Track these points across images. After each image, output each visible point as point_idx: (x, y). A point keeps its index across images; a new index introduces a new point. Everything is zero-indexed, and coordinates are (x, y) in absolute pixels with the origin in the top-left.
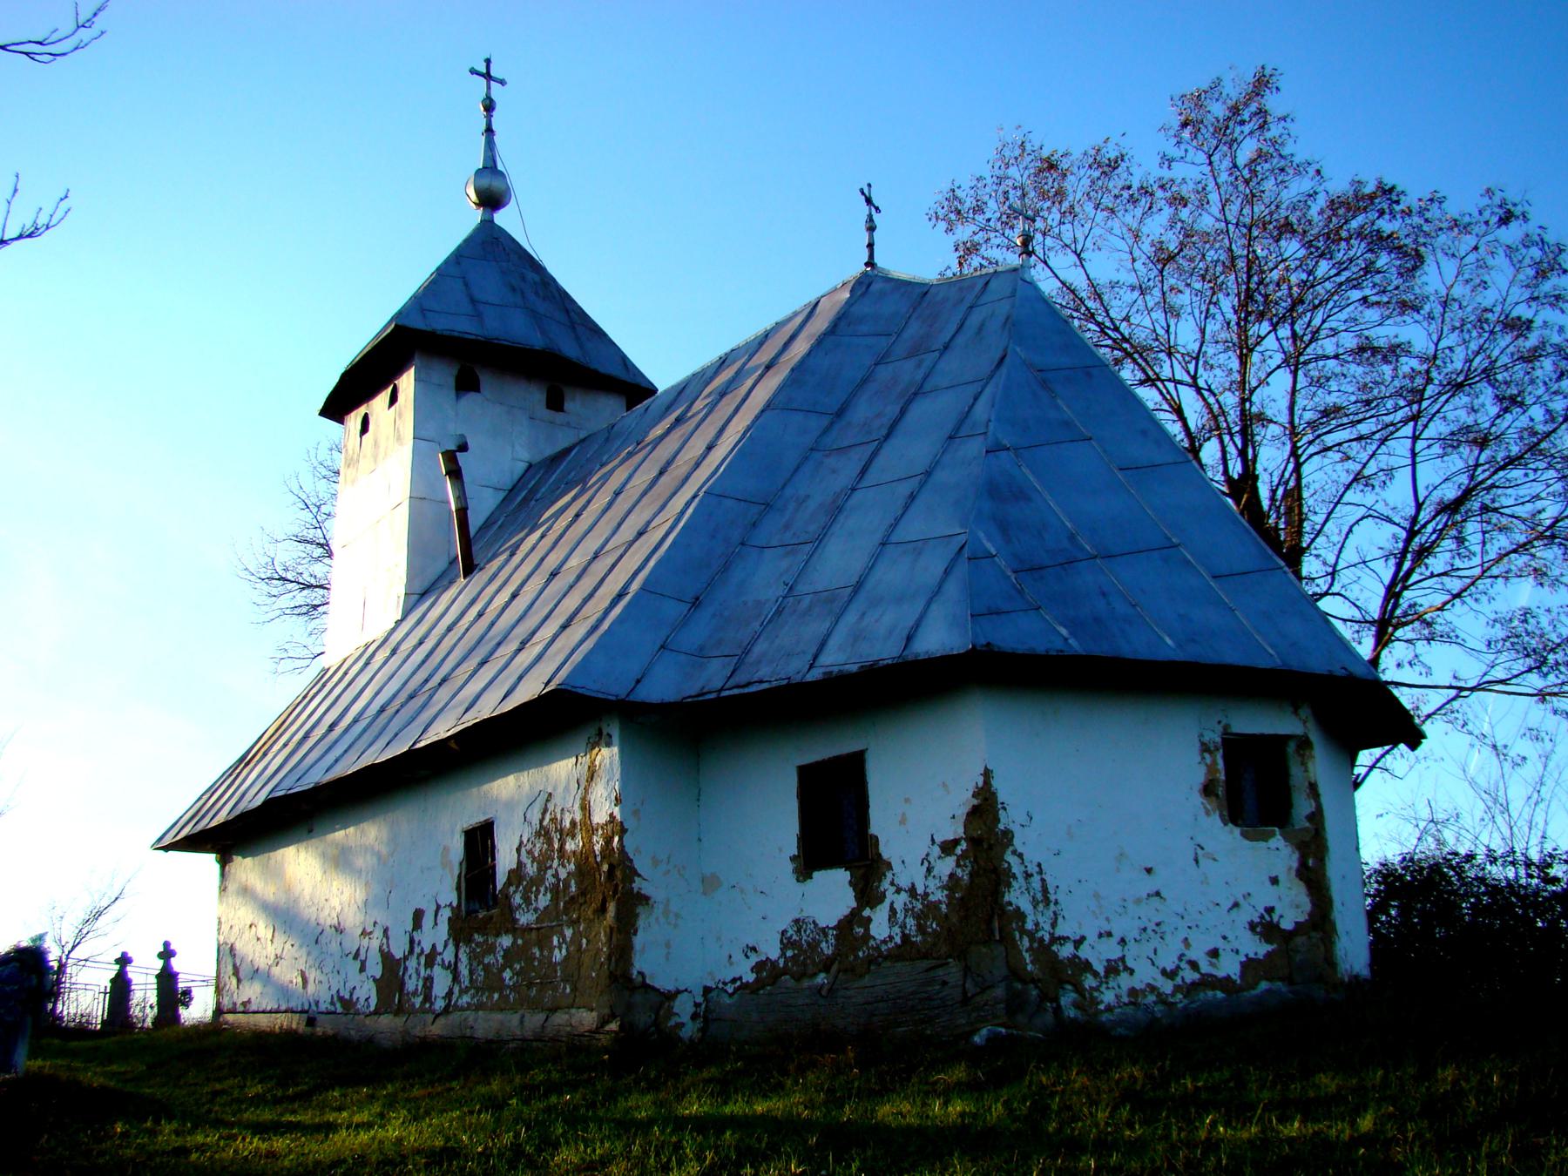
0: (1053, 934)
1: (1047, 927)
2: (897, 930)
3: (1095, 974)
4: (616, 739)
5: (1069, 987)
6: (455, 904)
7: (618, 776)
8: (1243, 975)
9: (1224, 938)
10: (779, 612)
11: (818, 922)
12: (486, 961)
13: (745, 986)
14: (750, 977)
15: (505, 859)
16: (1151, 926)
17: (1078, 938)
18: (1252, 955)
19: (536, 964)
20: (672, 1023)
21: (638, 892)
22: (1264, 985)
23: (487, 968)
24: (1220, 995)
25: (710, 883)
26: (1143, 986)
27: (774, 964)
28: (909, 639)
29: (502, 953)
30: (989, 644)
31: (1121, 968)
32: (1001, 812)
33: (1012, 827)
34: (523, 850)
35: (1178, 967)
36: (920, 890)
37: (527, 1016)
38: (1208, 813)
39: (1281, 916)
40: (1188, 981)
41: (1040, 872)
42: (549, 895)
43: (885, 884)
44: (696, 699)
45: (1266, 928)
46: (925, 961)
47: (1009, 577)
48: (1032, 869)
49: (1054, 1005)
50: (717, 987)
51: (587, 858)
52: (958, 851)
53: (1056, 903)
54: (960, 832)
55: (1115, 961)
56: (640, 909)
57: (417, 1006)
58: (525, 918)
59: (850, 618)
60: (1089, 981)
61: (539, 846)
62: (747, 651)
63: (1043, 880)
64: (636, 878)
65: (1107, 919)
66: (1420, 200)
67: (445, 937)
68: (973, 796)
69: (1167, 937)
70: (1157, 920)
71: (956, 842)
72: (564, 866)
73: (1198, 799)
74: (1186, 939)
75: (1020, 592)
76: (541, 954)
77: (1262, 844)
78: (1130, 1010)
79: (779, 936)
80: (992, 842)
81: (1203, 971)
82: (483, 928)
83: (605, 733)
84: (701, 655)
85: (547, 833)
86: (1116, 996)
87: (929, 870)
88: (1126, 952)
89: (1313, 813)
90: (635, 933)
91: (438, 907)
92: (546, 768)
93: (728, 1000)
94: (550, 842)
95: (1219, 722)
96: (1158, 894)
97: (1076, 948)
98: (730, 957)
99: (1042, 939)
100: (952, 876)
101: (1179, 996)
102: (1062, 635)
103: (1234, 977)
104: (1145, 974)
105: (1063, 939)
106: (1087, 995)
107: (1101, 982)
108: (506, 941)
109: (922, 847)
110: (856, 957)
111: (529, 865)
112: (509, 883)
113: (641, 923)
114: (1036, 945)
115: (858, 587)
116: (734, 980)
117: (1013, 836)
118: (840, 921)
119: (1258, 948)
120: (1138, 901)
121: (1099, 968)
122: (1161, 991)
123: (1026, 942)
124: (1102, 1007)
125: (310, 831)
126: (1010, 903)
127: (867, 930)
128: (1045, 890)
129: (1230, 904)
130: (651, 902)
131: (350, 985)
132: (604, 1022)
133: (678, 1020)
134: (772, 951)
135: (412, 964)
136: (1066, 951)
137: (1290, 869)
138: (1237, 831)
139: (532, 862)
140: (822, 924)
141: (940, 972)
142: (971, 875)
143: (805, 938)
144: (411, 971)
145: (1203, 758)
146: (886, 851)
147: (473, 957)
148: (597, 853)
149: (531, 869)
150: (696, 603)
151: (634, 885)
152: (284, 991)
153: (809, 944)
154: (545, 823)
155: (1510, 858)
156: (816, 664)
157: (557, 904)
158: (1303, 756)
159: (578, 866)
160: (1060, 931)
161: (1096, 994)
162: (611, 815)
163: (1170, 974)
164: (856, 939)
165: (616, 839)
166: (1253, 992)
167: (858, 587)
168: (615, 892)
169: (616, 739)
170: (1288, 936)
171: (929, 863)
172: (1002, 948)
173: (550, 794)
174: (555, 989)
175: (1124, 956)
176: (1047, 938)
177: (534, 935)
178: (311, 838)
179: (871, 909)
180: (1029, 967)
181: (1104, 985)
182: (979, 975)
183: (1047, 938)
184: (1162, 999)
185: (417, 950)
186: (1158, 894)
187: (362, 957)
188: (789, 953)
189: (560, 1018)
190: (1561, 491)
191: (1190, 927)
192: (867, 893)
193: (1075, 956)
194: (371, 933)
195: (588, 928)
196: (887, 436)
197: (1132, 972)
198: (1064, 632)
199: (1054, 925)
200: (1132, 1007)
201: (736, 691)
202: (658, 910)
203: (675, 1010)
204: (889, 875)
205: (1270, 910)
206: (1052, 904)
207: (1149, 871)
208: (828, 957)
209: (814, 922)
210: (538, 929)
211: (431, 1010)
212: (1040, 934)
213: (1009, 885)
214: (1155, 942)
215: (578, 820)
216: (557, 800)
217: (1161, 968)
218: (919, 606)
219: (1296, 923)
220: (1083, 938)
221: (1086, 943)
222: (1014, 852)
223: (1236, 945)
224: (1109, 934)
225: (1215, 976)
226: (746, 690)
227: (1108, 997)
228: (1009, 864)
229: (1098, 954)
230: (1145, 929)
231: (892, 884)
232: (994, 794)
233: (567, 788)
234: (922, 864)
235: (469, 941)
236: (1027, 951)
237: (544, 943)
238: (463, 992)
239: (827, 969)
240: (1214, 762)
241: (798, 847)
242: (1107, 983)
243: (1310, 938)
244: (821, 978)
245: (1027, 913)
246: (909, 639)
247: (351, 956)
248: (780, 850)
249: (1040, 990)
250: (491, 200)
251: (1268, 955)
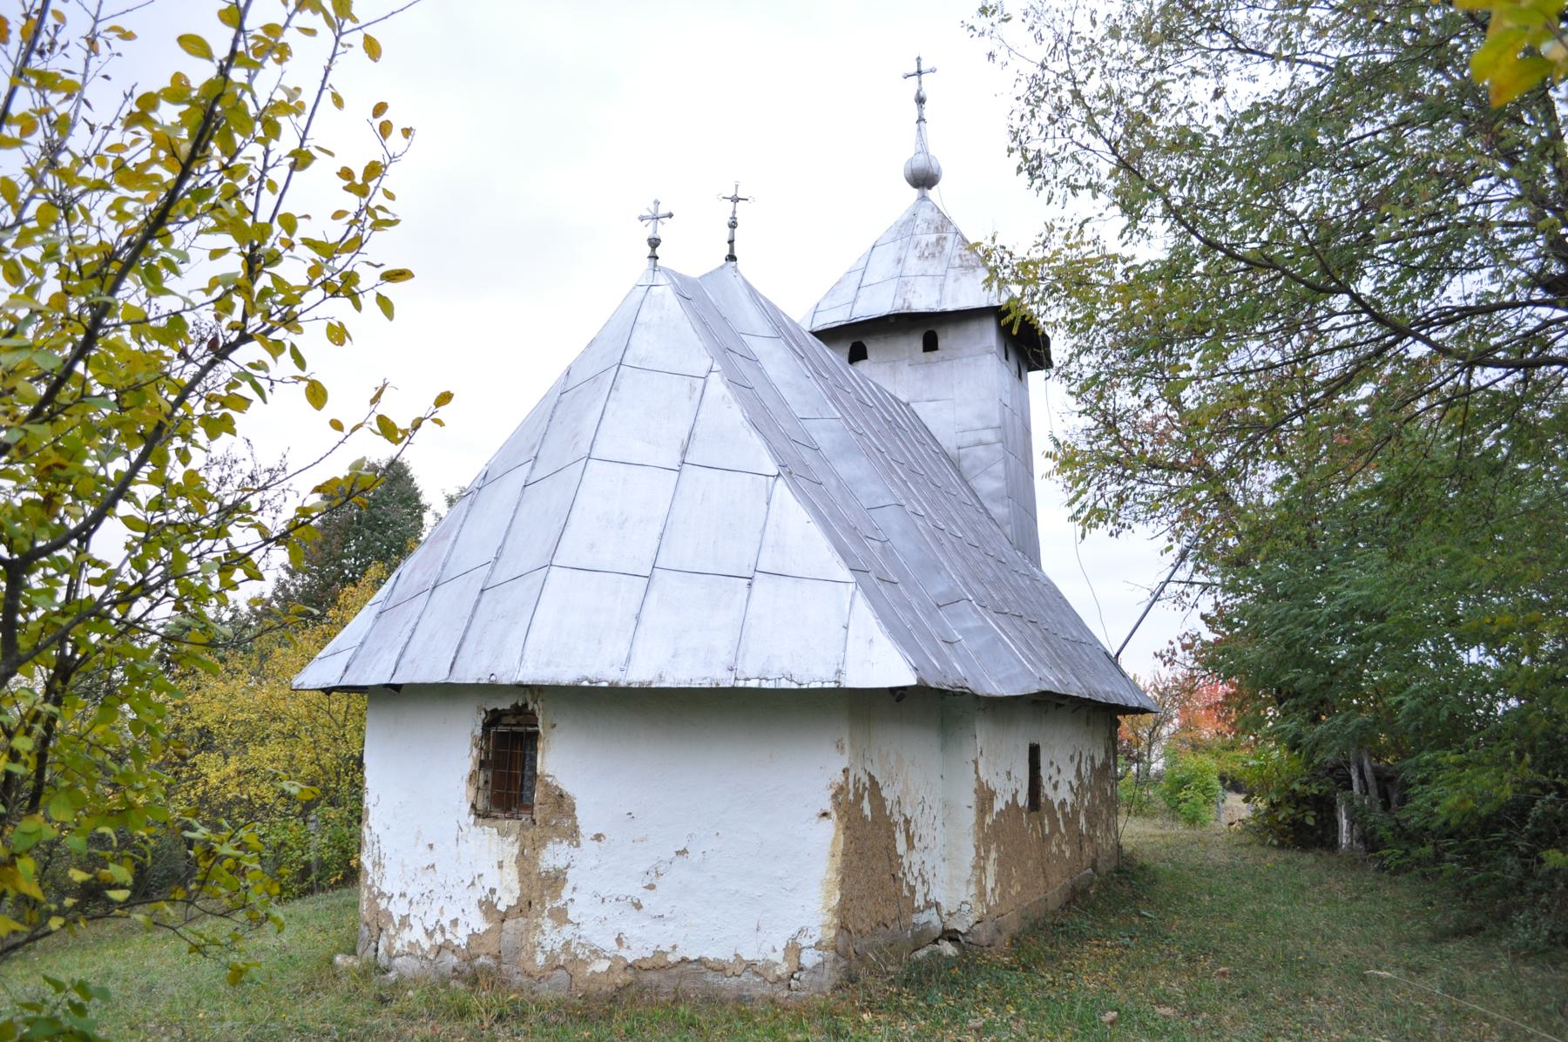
16: (427, 892)
119: (479, 924)
123: (366, 894)
160: (385, 889)
186: (433, 866)
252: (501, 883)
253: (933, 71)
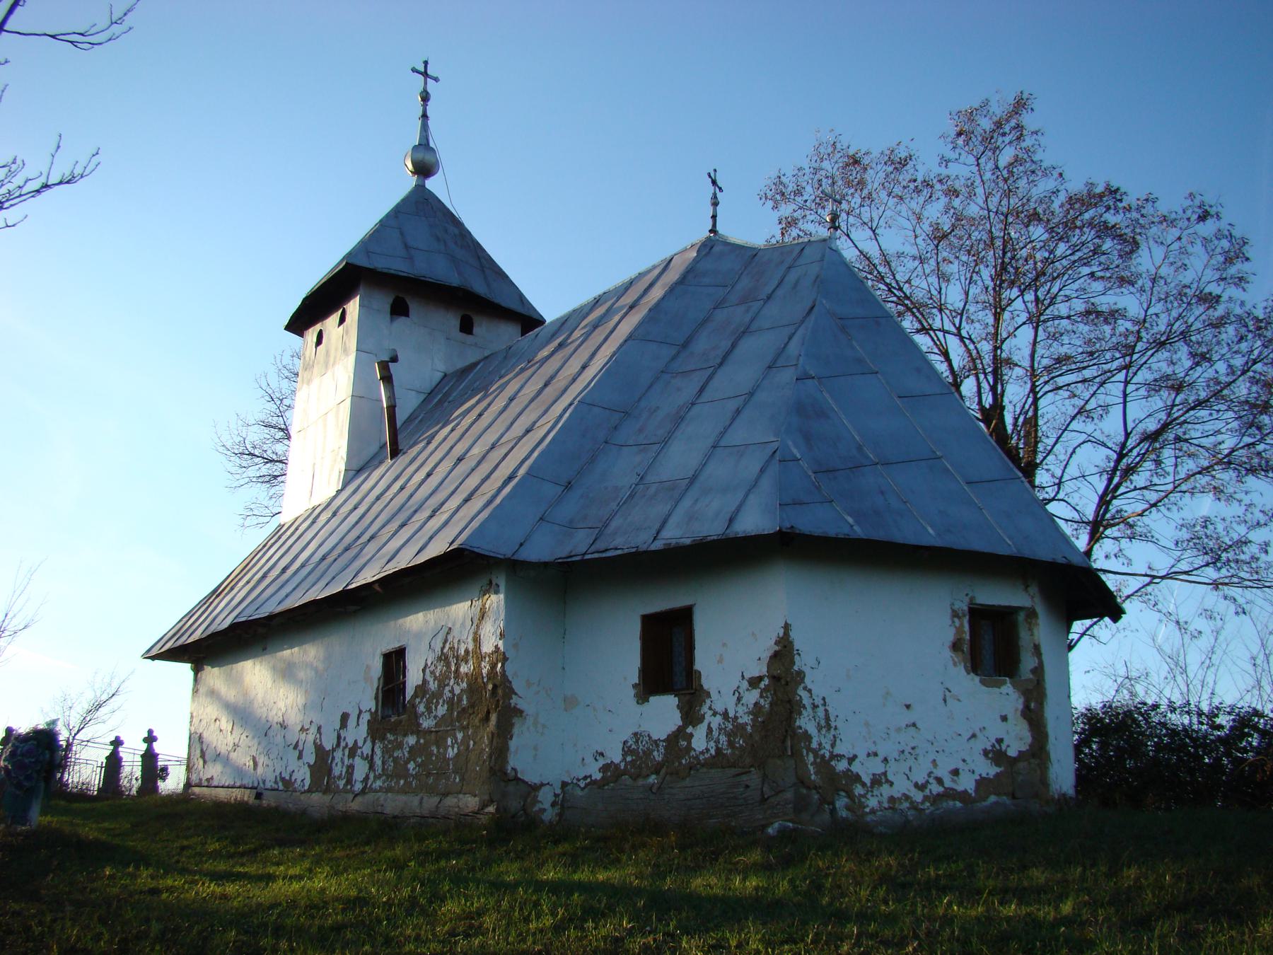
0: (832, 752)
1: (828, 747)
2: (712, 744)
3: (864, 784)
4: (502, 588)
5: (843, 794)
6: (373, 710)
7: (502, 616)
8: (976, 790)
9: (964, 761)
10: (632, 496)
11: (651, 735)
12: (395, 755)
13: (594, 782)
14: (598, 776)
15: (413, 677)
16: (908, 749)
17: (851, 756)
18: (984, 775)
19: (434, 758)
20: (536, 809)
21: (515, 707)
22: (993, 798)
23: (396, 760)
24: (958, 804)
25: (570, 703)
26: (900, 795)
27: (617, 766)
28: (731, 520)
29: (408, 749)
30: (792, 527)
31: (883, 781)
32: (796, 657)
33: (804, 669)
34: (428, 671)
35: (927, 782)
36: (731, 714)
37: (425, 799)
38: (955, 664)
39: (1008, 746)
40: (934, 793)
41: (825, 704)
42: (446, 706)
43: (705, 709)
44: (565, 560)
45: (996, 754)
46: (733, 769)
47: (810, 476)
48: (818, 701)
49: (831, 807)
50: (572, 782)
51: (476, 679)
52: (762, 685)
53: (836, 728)
54: (764, 671)
55: (879, 775)
56: (515, 720)
57: (341, 787)
58: (427, 723)
59: (686, 503)
60: (859, 790)
61: (440, 668)
62: (606, 525)
63: (826, 711)
64: (513, 696)
65: (874, 742)
66: (1138, 199)
67: (365, 735)
68: (775, 644)
69: (921, 758)
70: (913, 745)
71: (760, 679)
72: (458, 684)
73: (948, 653)
74: (934, 760)
75: (818, 488)
76: (438, 751)
77: (996, 690)
78: (889, 813)
79: (621, 745)
80: (788, 679)
81: (946, 786)
82: (393, 730)
83: (494, 583)
84: (571, 526)
85: (447, 658)
86: (879, 802)
87: (739, 699)
88: (888, 769)
89: (1036, 668)
90: (511, 738)
91: (361, 712)
92: (447, 608)
93: (579, 792)
94: (448, 665)
95: (967, 595)
96: (914, 725)
97: (850, 764)
98: (583, 759)
99: (823, 756)
100: (756, 704)
101: (928, 804)
102: (849, 523)
103: (970, 791)
104: (901, 786)
105: (839, 757)
106: (857, 801)
107: (868, 791)
108: (411, 740)
109: (735, 681)
110: (680, 763)
111: (431, 683)
112: (415, 695)
113: (516, 730)
114: (818, 760)
115: (693, 479)
116: (585, 778)
117: (805, 676)
118: (669, 736)
119: (989, 770)
120: (898, 730)
121: (867, 779)
122: (914, 799)
123: (811, 758)
124: (867, 810)
125: (264, 649)
126: (800, 727)
127: (689, 743)
128: (827, 718)
129: (969, 735)
130: (524, 714)
131: (290, 769)
132: (484, 805)
133: (541, 806)
134: (616, 756)
135: (338, 754)
136: (841, 766)
137: (1016, 710)
138: (977, 679)
139: (434, 680)
140: (655, 737)
141: (744, 778)
142: (771, 704)
143: (641, 747)
144: (338, 760)
145: (953, 622)
146: (706, 683)
147: (386, 751)
148: (484, 675)
149: (433, 686)
150: (569, 486)
151: (511, 701)
152: (239, 771)
153: (644, 752)
154: (445, 651)
155: (1186, 708)
156: (658, 537)
157: (452, 713)
158: (1030, 624)
159: (469, 685)
161: (863, 800)
162: (496, 647)
163: (921, 787)
164: (681, 750)
165: (500, 665)
166: (984, 803)
167: (693, 479)
168: (497, 706)
169: (502, 588)
170: (1014, 761)
171: (739, 693)
172: (793, 761)
173: (450, 629)
174: (448, 779)
175: (886, 772)
176: (827, 755)
177: (433, 736)
178: (266, 654)
179: (693, 727)
180: (813, 777)
181: (870, 794)
182: (774, 782)
183: (827, 755)
184: (914, 806)
185: (343, 744)
186: (914, 725)
187: (300, 747)
188: (629, 759)
189: (450, 801)
190: (1237, 428)
191: (937, 752)
192: (691, 715)
193: (849, 770)
194: (308, 729)
195: (475, 733)
196: (721, 364)
197: (891, 784)
198: (850, 520)
199: (833, 745)
200: (890, 811)
201: (596, 555)
202: (530, 721)
203: (539, 799)
204: (708, 701)
205: (1000, 741)
206: (832, 729)
207: (908, 707)
208: (658, 763)
209: (649, 735)
210: (437, 732)
211: (351, 791)
212: (822, 752)
213: (800, 714)
214: (911, 762)
215: (470, 650)
216: (455, 633)
217: (914, 781)
218: (740, 495)
219: (1019, 751)
220: (855, 757)
221: (857, 760)
222: (805, 688)
223: (972, 766)
224: (876, 754)
225: (956, 790)
226: (604, 555)
227: (872, 802)
228: (801, 697)
229: (865, 769)
230: (903, 752)
231: (710, 708)
232: (791, 643)
233: (463, 624)
234: (734, 694)
235: (383, 738)
236: (811, 764)
237: (440, 742)
238: (377, 777)
239: (657, 773)
240: (962, 625)
241: (639, 677)
242: (872, 792)
243: (1029, 763)
244: (653, 779)
245: (813, 735)
246: (731, 520)
247: (292, 747)
248: (625, 679)
249: (821, 796)
250: (424, 169)
251: (997, 775)
252: (1008, 732)
253: (426, 63)
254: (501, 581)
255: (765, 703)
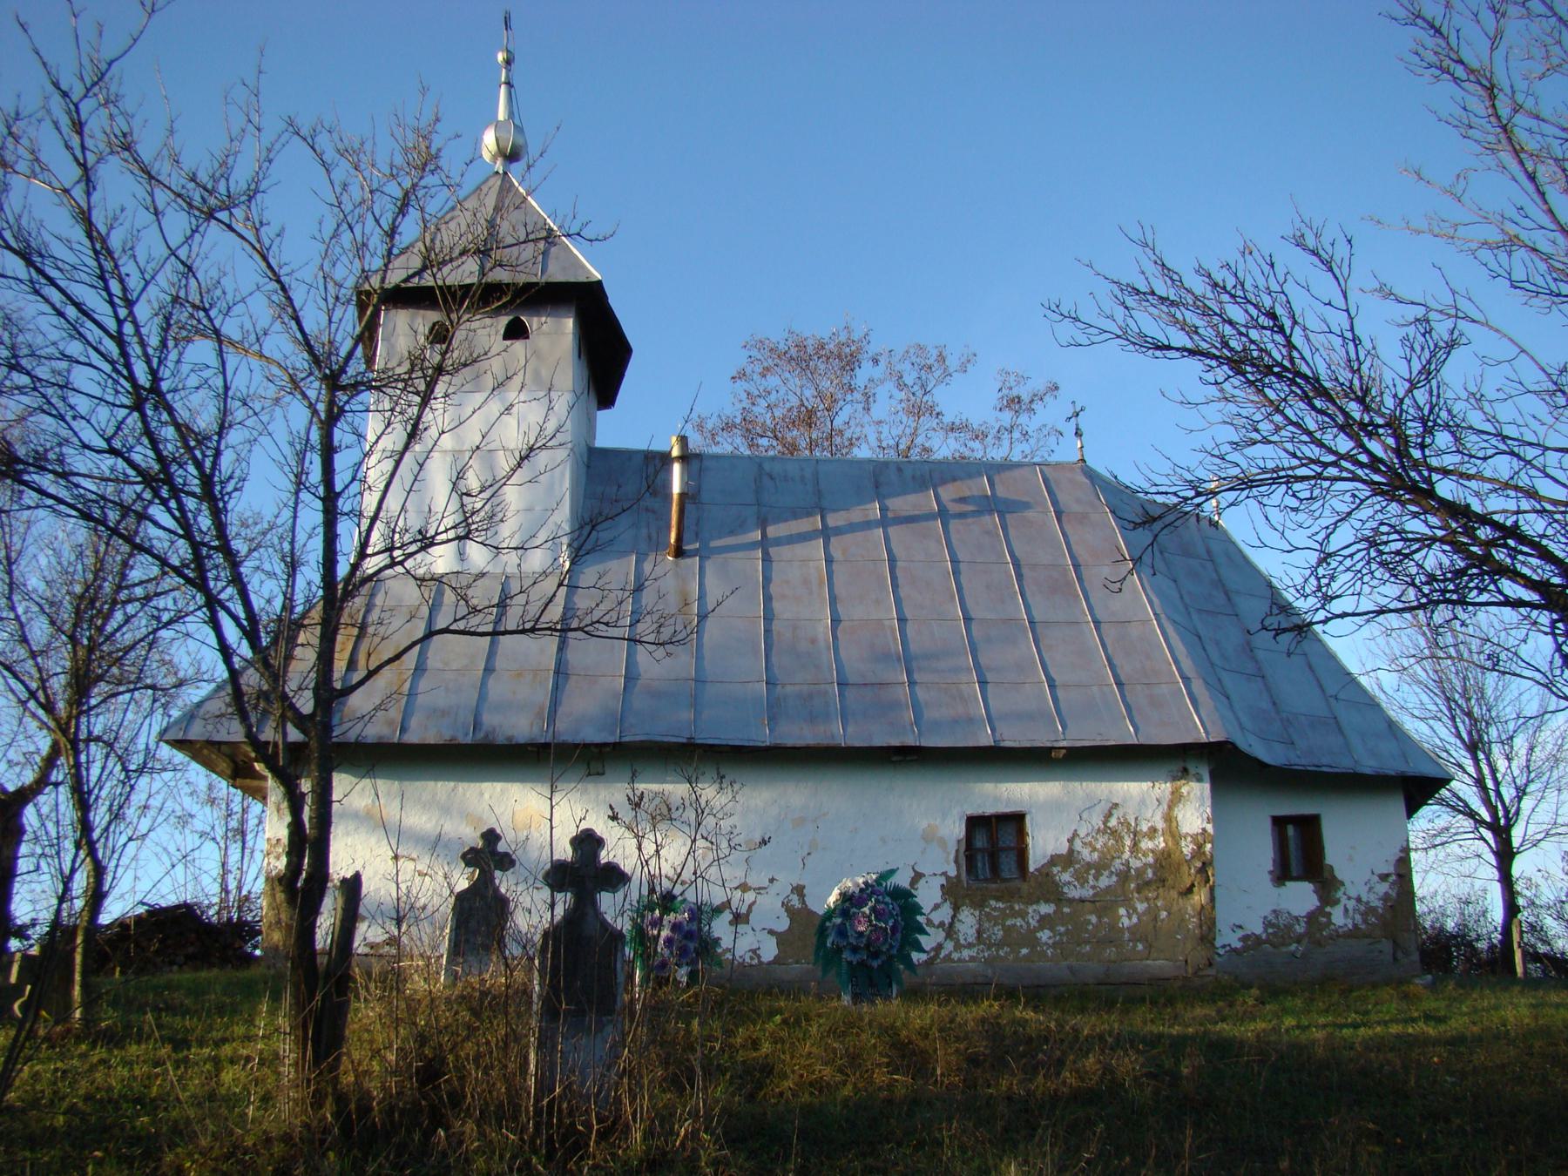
4: (1206, 776)
12: (1009, 923)
13: (1235, 950)
14: (1239, 945)
27: (1258, 937)
36: (1364, 899)
43: (1340, 894)
54: (1391, 870)
71: (1388, 875)
87: (1371, 889)
108: (1046, 909)
140: (1295, 913)
142: (1398, 894)
146: (1339, 874)
188: (1270, 930)
208: (1300, 934)
235: (979, 904)
239: (1298, 942)
254: (1205, 772)
255: (1393, 894)
